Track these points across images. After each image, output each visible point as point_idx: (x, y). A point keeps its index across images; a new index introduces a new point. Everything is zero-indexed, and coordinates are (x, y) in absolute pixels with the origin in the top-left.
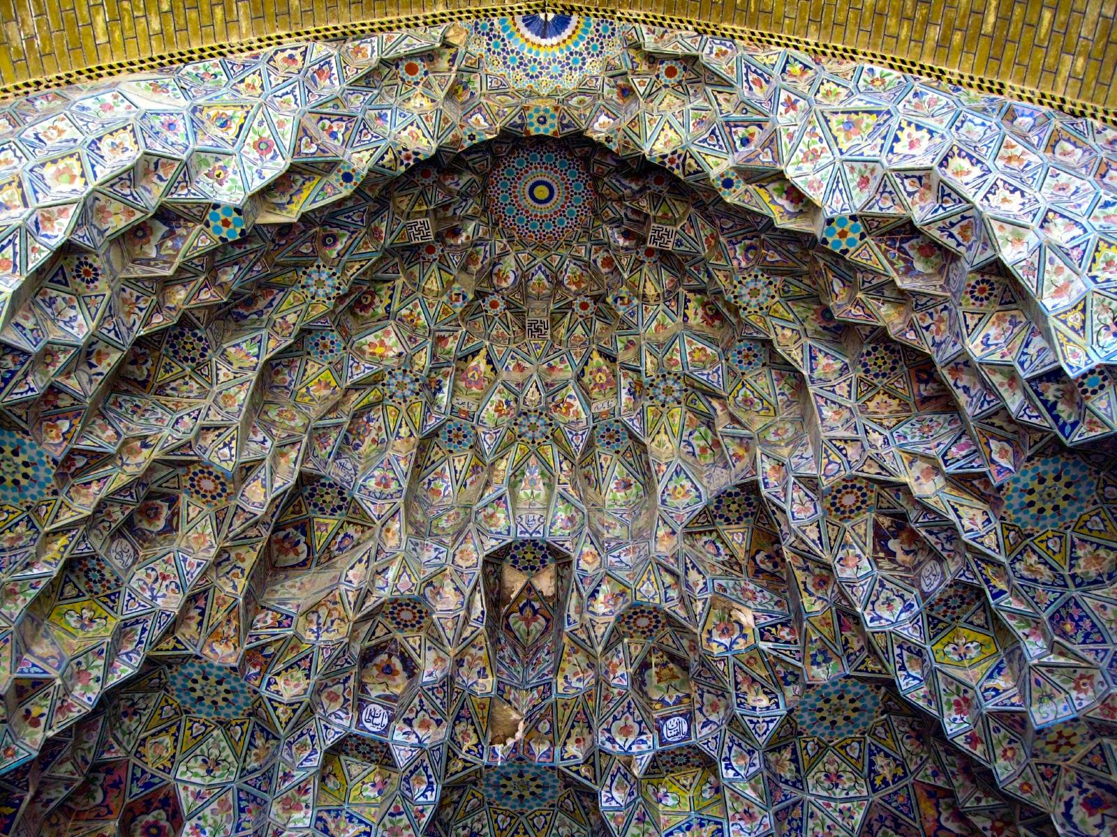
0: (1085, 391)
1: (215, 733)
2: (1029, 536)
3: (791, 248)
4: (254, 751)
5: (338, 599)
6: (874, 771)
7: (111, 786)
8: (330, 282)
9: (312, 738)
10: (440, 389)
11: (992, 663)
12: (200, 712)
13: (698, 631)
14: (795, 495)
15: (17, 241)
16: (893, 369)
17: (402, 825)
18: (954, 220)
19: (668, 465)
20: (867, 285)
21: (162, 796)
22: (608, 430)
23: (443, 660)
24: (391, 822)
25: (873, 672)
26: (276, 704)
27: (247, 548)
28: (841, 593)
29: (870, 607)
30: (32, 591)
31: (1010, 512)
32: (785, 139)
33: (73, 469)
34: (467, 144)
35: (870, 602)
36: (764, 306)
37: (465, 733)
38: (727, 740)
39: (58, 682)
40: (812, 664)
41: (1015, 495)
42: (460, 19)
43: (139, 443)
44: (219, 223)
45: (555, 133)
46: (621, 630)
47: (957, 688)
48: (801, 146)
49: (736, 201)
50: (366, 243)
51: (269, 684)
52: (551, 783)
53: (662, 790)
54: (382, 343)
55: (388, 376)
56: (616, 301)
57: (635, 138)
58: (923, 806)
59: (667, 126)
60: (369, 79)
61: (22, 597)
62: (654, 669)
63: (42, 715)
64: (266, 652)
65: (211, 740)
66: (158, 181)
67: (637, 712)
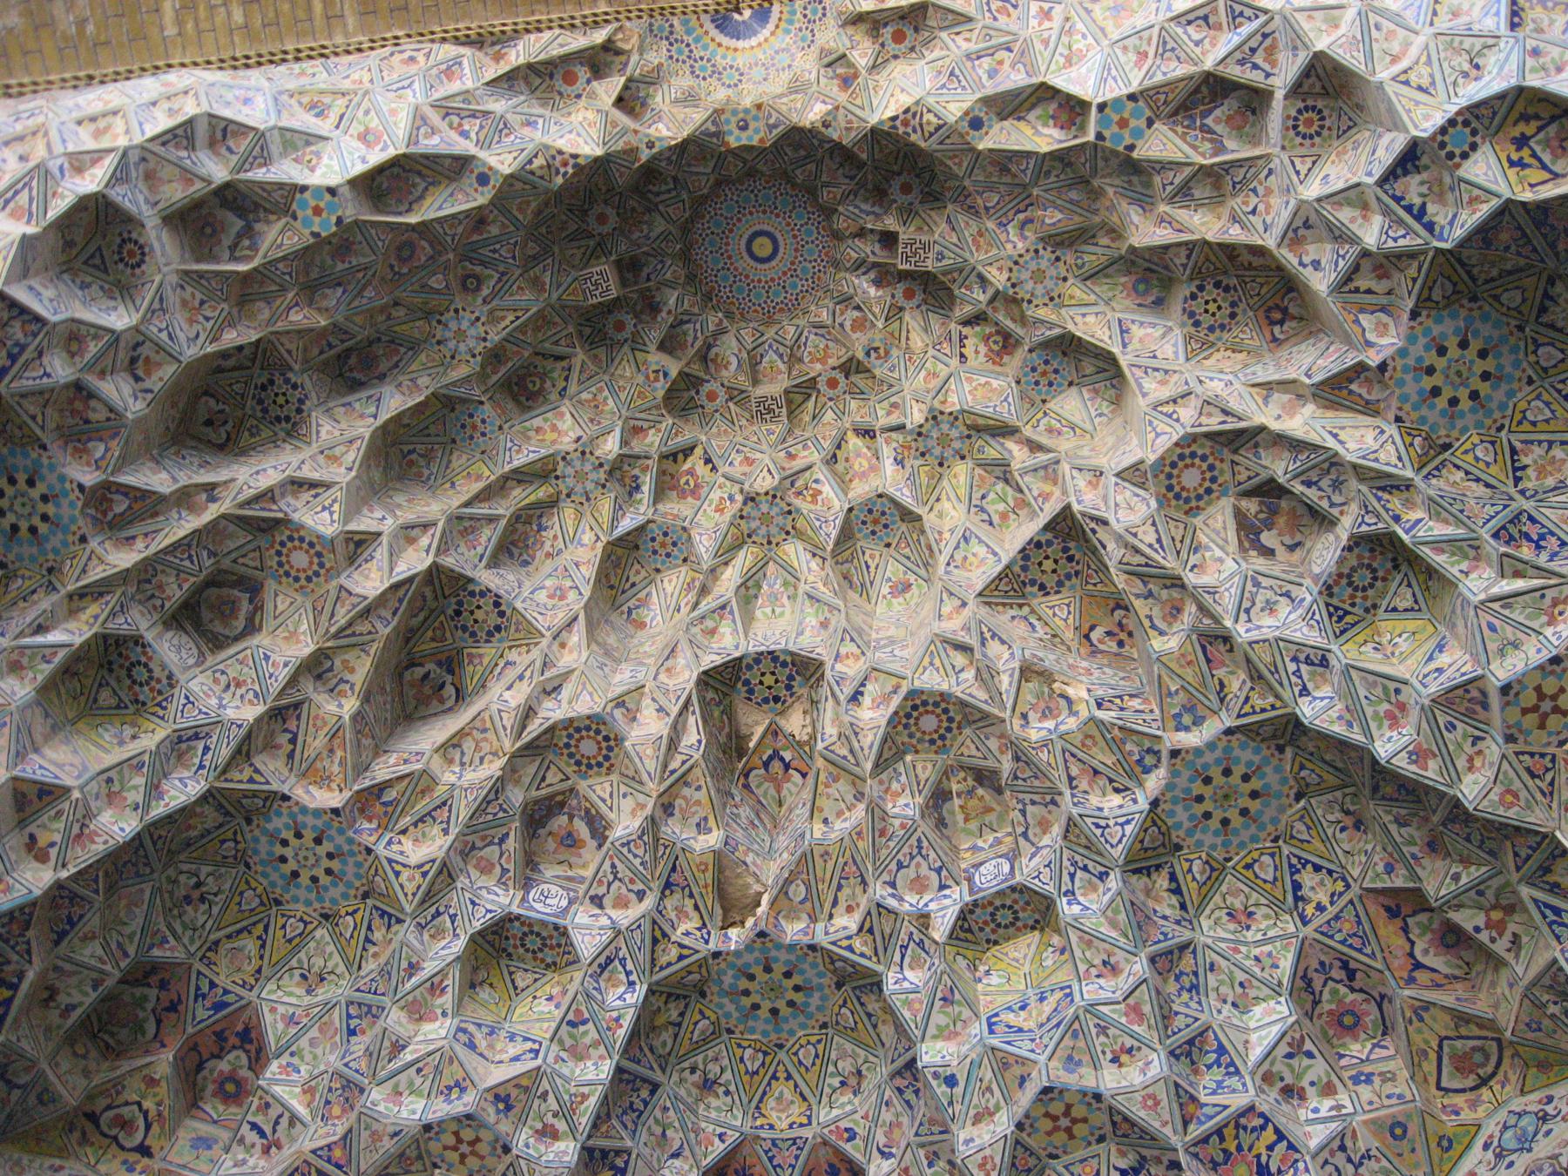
0: (1451, 156)
1: (319, 933)
2: (1446, 447)
3: (1074, 195)
4: (372, 949)
5: (489, 725)
6: (1302, 899)
7: (167, 1009)
8: (472, 332)
9: (453, 918)
10: (638, 488)
11: (1431, 645)
12: (296, 899)
13: (1007, 715)
14: (1119, 499)
15: (34, 183)
16: (1233, 316)
17: (587, 1040)
18: (1253, 43)
19: (952, 531)
20: (1169, 188)
21: (240, 1028)
22: (870, 511)
23: (643, 806)
24: (571, 1036)
25: (1263, 710)
26: (398, 868)
27: (356, 652)
28: (1201, 608)
29: (1243, 616)
30: (45, 666)
31: (1407, 407)
32: (1039, 46)
33: (110, 515)
34: (645, 155)
35: (1244, 610)
36: (1055, 295)
37: (680, 911)
38: (1066, 863)
39: (76, 794)
40: (1177, 730)
41: (1409, 378)
42: (629, 19)
43: (204, 496)
44: (309, 212)
45: (761, 140)
46: (899, 740)
47: (1385, 688)
48: (1060, 49)
49: (990, 145)
50: (520, 288)
51: (390, 843)
52: (816, 981)
53: (982, 968)
54: (554, 428)
55: (562, 464)
56: (868, 354)
57: (858, 112)
58: (1382, 932)
59: (897, 91)
60: (509, 81)
61: (31, 675)
62: (957, 802)
63: (52, 845)
64: (386, 798)
65: (312, 944)
66: (227, 154)
67: (932, 855)
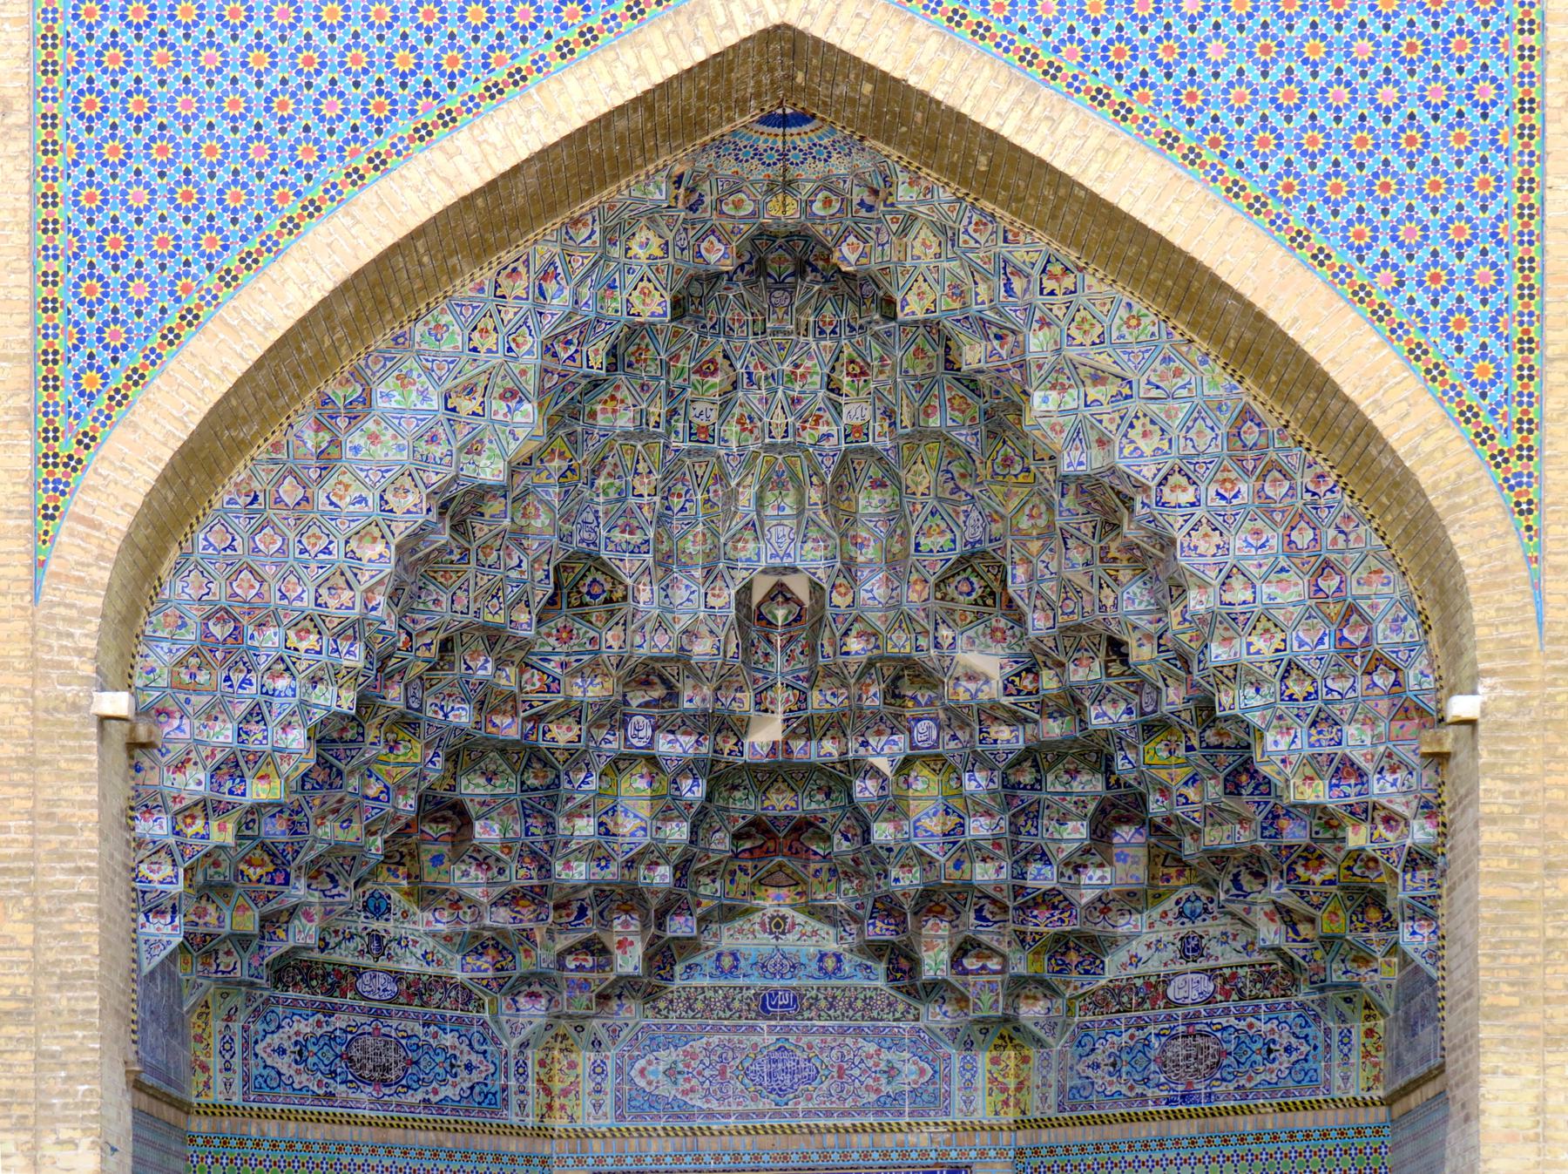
32: (1034, 368)
59: (921, 279)
